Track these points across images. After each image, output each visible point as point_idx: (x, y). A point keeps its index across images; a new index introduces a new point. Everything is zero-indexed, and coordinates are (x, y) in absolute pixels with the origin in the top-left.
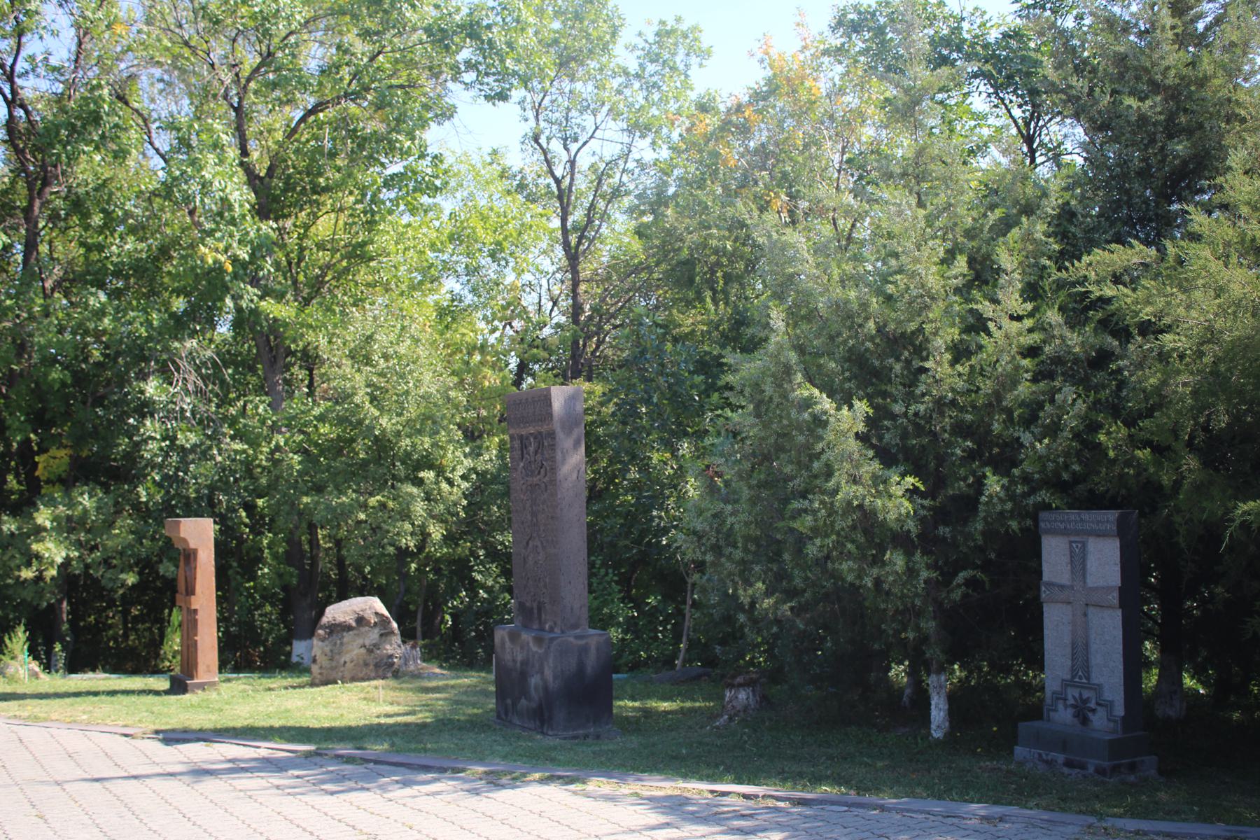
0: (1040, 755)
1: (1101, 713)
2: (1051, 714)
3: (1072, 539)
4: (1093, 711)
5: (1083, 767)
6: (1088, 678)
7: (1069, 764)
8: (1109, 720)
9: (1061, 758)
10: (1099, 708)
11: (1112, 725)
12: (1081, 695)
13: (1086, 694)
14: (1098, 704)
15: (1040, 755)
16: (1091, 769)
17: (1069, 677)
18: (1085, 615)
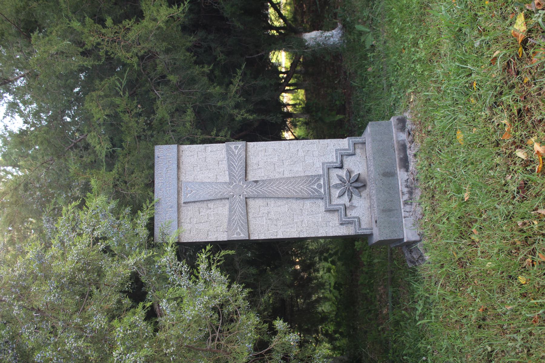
0: (406, 203)
1: (349, 163)
2: (364, 226)
3: (182, 201)
4: (349, 172)
5: (403, 148)
6: (319, 177)
7: (405, 163)
8: (354, 154)
9: (402, 175)
10: (345, 167)
11: (358, 151)
12: (336, 186)
13: (335, 181)
14: (341, 167)
15: (406, 203)
16: (403, 136)
17: (321, 203)
18: (256, 182)
